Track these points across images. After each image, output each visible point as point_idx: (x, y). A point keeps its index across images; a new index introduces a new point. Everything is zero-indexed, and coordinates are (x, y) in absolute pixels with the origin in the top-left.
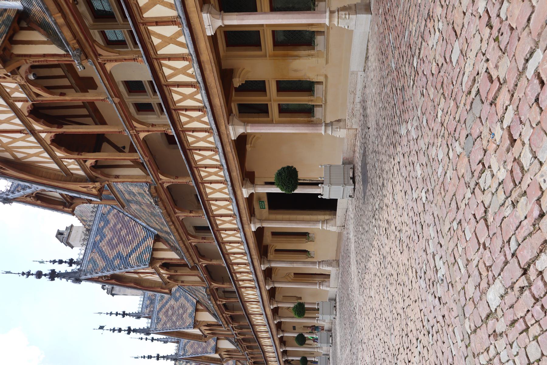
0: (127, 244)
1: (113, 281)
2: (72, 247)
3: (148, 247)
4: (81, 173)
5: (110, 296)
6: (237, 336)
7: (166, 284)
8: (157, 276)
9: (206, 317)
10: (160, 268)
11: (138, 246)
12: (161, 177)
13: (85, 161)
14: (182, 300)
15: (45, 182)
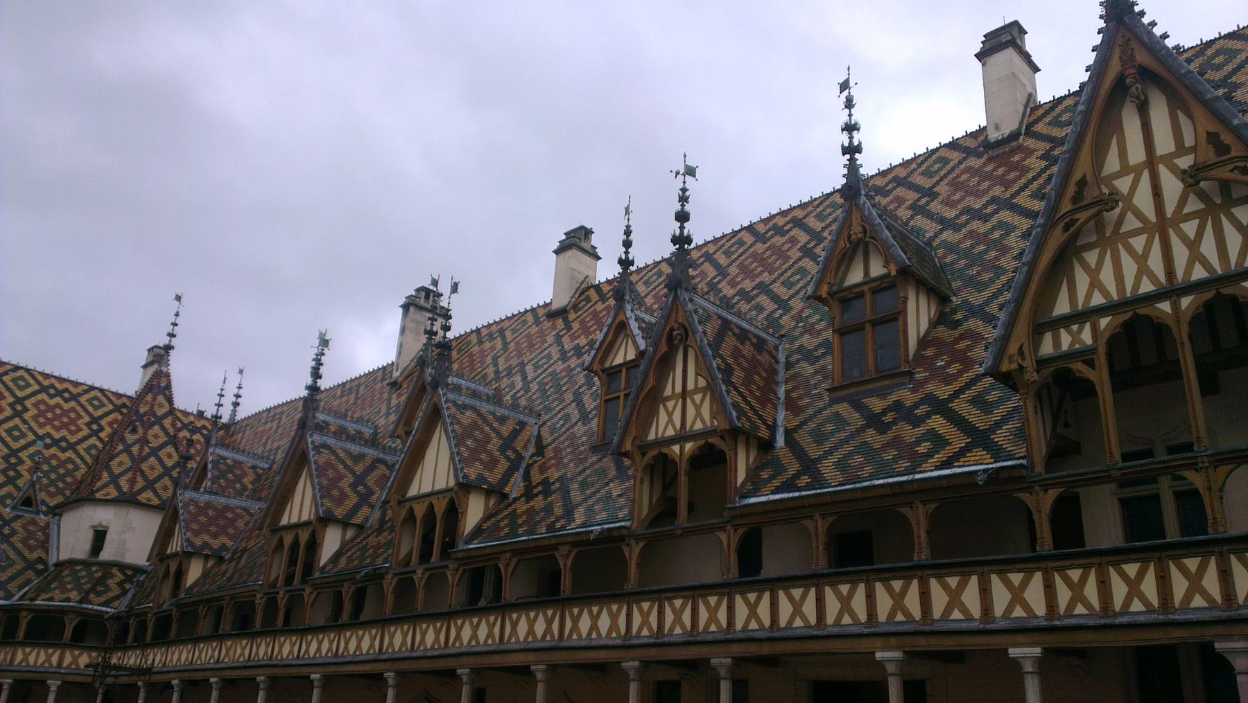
0: (748, 382)
1: (664, 348)
2: (557, 252)
3: (758, 428)
4: (1047, 348)
5: (403, 301)
6: (396, 574)
7: (640, 447)
8: (670, 432)
9: (475, 511)
10: (702, 442)
11: (752, 407)
12: (1052, 494)
13: (1090, 363)
14: (504, 465)
15: (1033, 288)
